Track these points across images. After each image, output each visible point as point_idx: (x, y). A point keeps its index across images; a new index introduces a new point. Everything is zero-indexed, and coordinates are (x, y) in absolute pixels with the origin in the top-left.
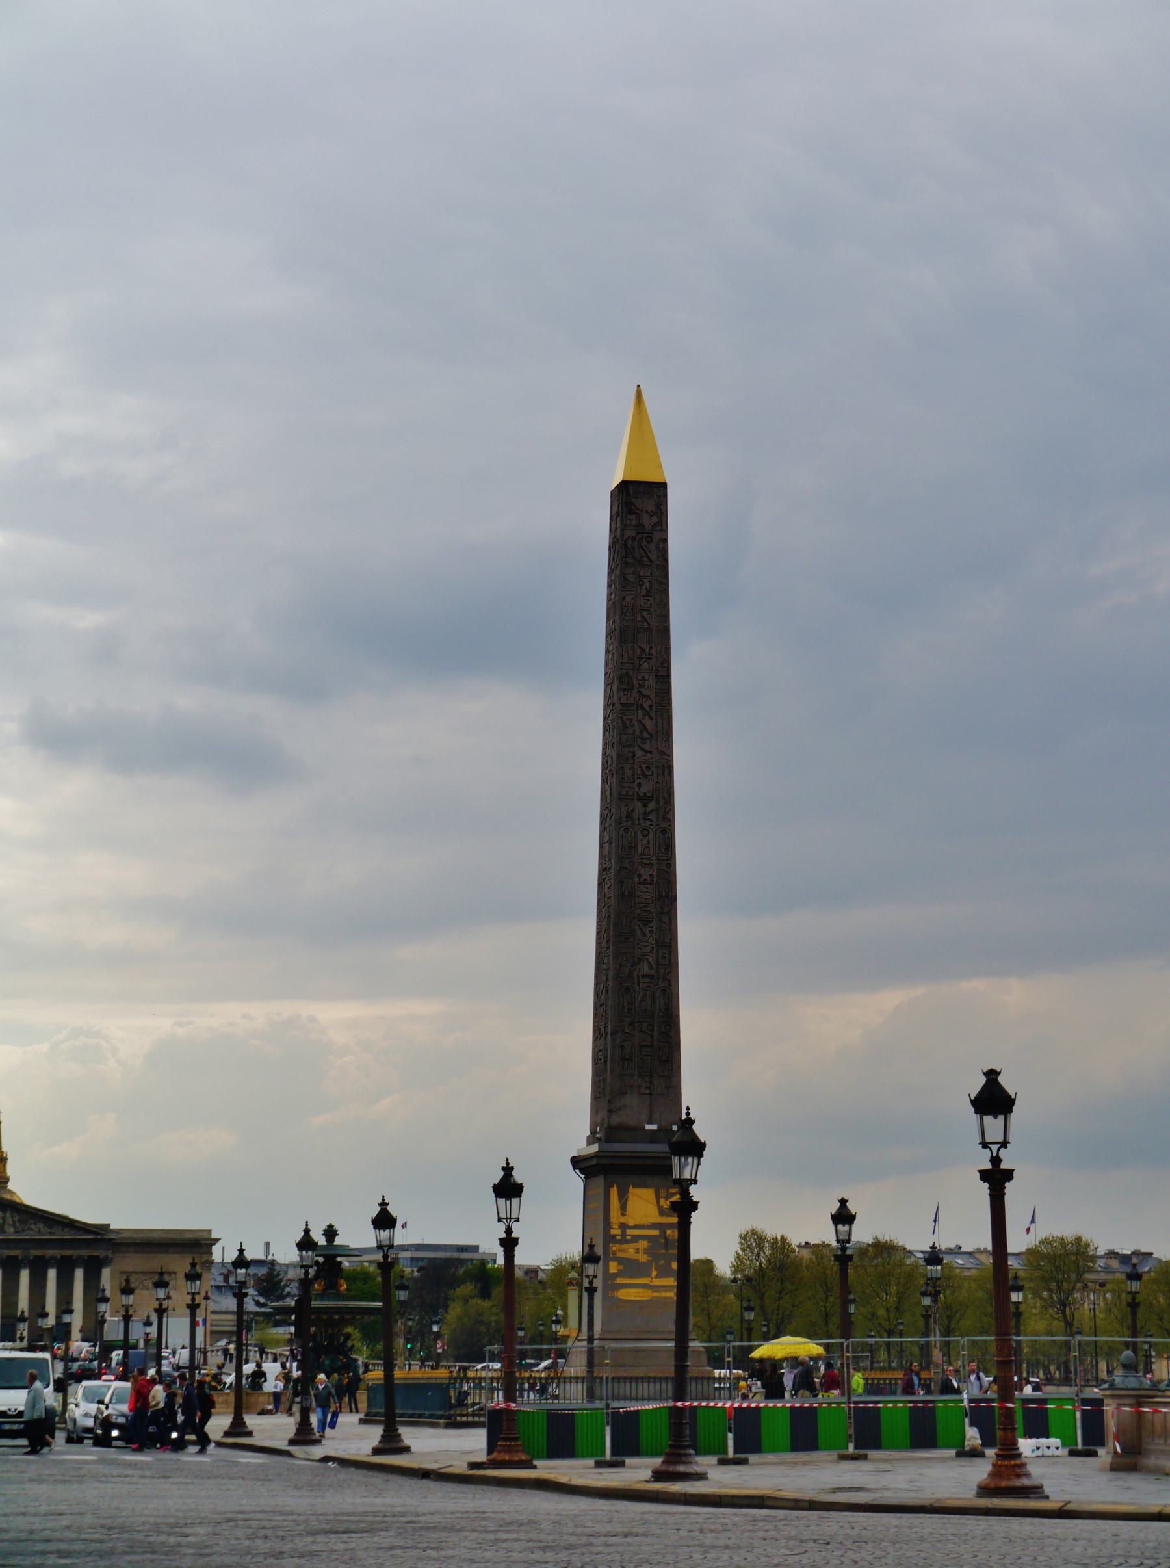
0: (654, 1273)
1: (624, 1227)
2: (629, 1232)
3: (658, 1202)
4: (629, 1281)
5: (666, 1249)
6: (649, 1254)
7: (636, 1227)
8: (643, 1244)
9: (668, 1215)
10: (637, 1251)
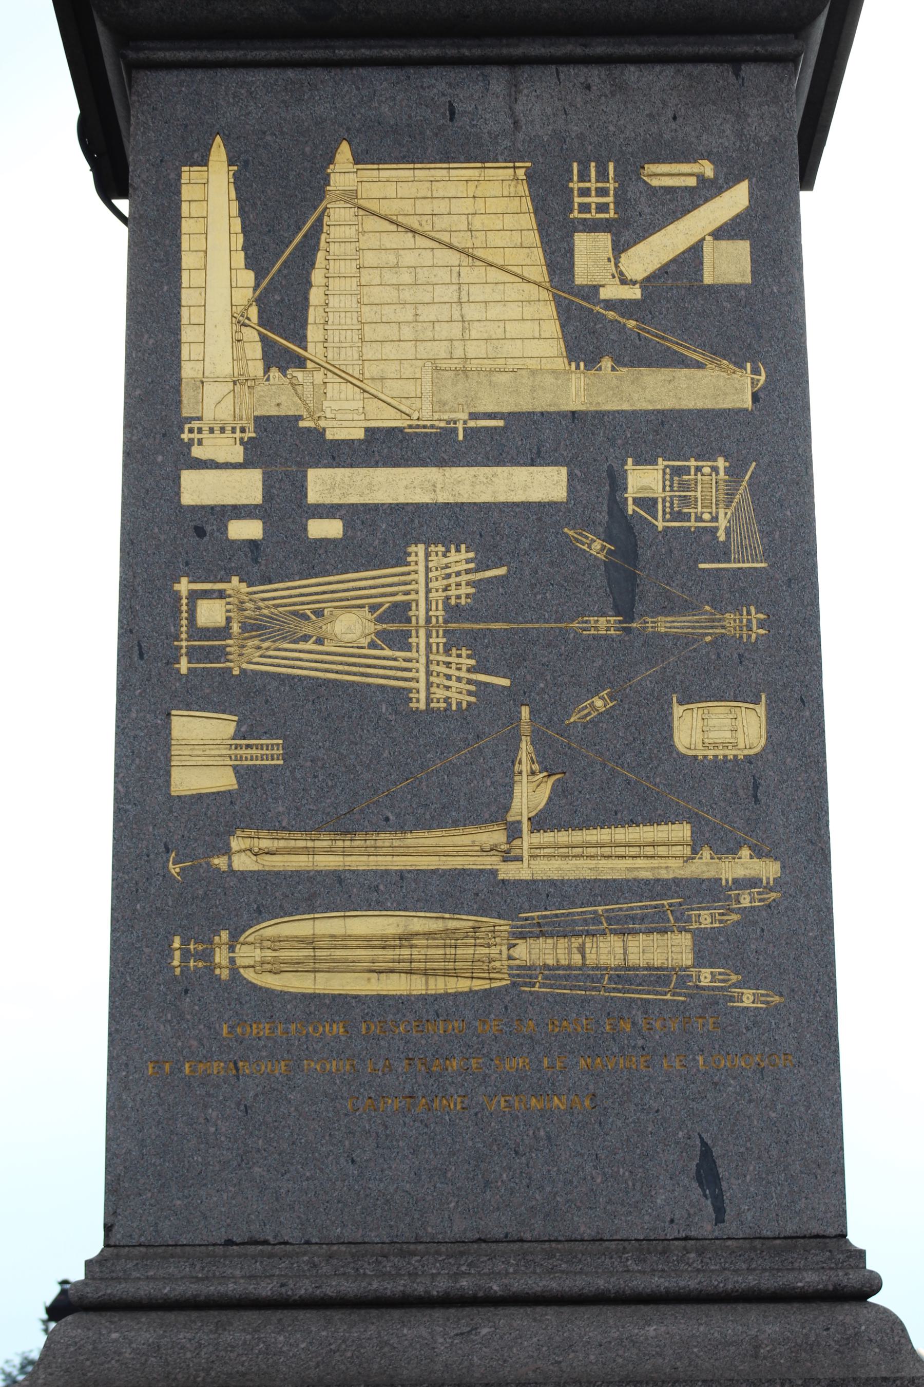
0: (530, 794)
1: (284, 448)
2: (323, 484)
3: (559, 262)
4: (325, 855)
5: (626, 609)
6: (486, 656)
7: (385, 447)
8: (439, 575)
9: (639, 355)
10: (394, 624)
